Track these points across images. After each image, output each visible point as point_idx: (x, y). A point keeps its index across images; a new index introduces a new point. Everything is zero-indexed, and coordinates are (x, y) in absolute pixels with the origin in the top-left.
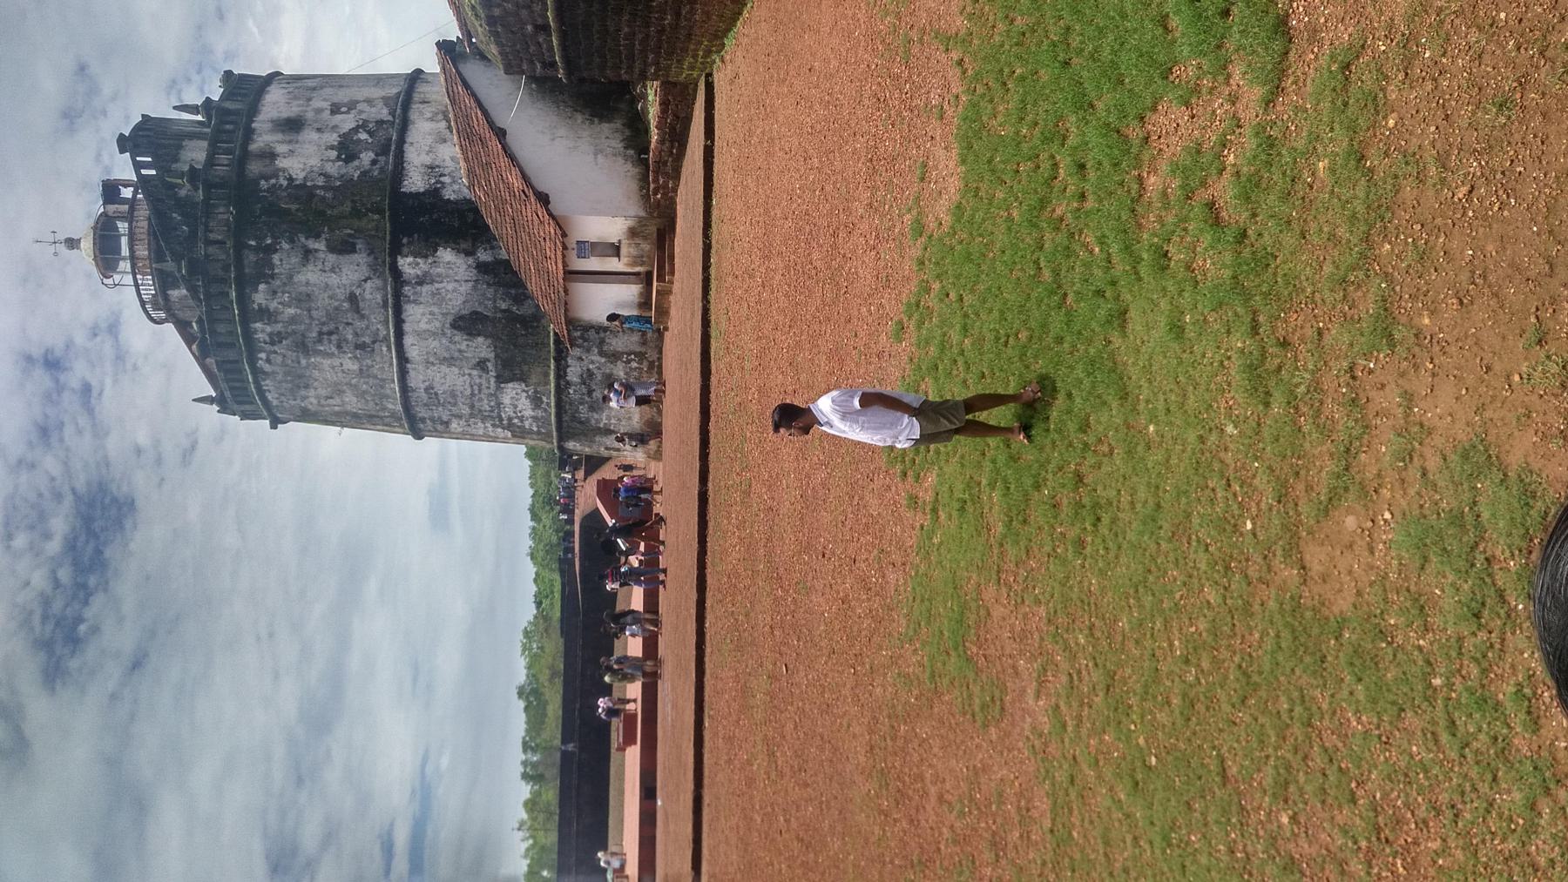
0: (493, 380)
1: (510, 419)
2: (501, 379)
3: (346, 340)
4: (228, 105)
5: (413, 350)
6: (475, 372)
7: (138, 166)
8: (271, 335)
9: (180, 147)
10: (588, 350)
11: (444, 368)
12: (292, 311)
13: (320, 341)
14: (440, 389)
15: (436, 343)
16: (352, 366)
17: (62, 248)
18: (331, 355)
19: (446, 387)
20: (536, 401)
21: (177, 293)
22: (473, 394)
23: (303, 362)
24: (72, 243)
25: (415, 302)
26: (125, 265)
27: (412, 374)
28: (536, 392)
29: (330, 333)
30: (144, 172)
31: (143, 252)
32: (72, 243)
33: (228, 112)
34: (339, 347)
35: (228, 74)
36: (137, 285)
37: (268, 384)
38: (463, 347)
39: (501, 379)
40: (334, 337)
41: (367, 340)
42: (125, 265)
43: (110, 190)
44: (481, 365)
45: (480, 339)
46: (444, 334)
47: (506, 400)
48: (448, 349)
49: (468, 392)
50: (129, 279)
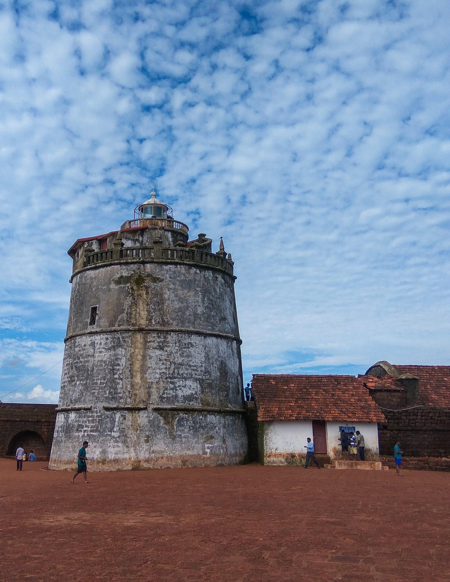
0: (200, 377)
2: (201, 382)
3: (211, 311)
5: (210, 341)
6: (203, 369)
8: (208, 278)
11: (203, 354)
13: (209, 299)
14: (192, 350)
15: (215, 353)
16: (200, 310)
18: (203, 301)
19: (193, 353)
22: (190, 366)
23: (198, 289)
25: (227, 346)
27: (199, 338)
29: (213, 305)
38: (215, 365)
44: (207, 372)
45: (219, 374)
46: (219, 357)
47: (188, 383)
48: (213, 358)
49: (191, 363)
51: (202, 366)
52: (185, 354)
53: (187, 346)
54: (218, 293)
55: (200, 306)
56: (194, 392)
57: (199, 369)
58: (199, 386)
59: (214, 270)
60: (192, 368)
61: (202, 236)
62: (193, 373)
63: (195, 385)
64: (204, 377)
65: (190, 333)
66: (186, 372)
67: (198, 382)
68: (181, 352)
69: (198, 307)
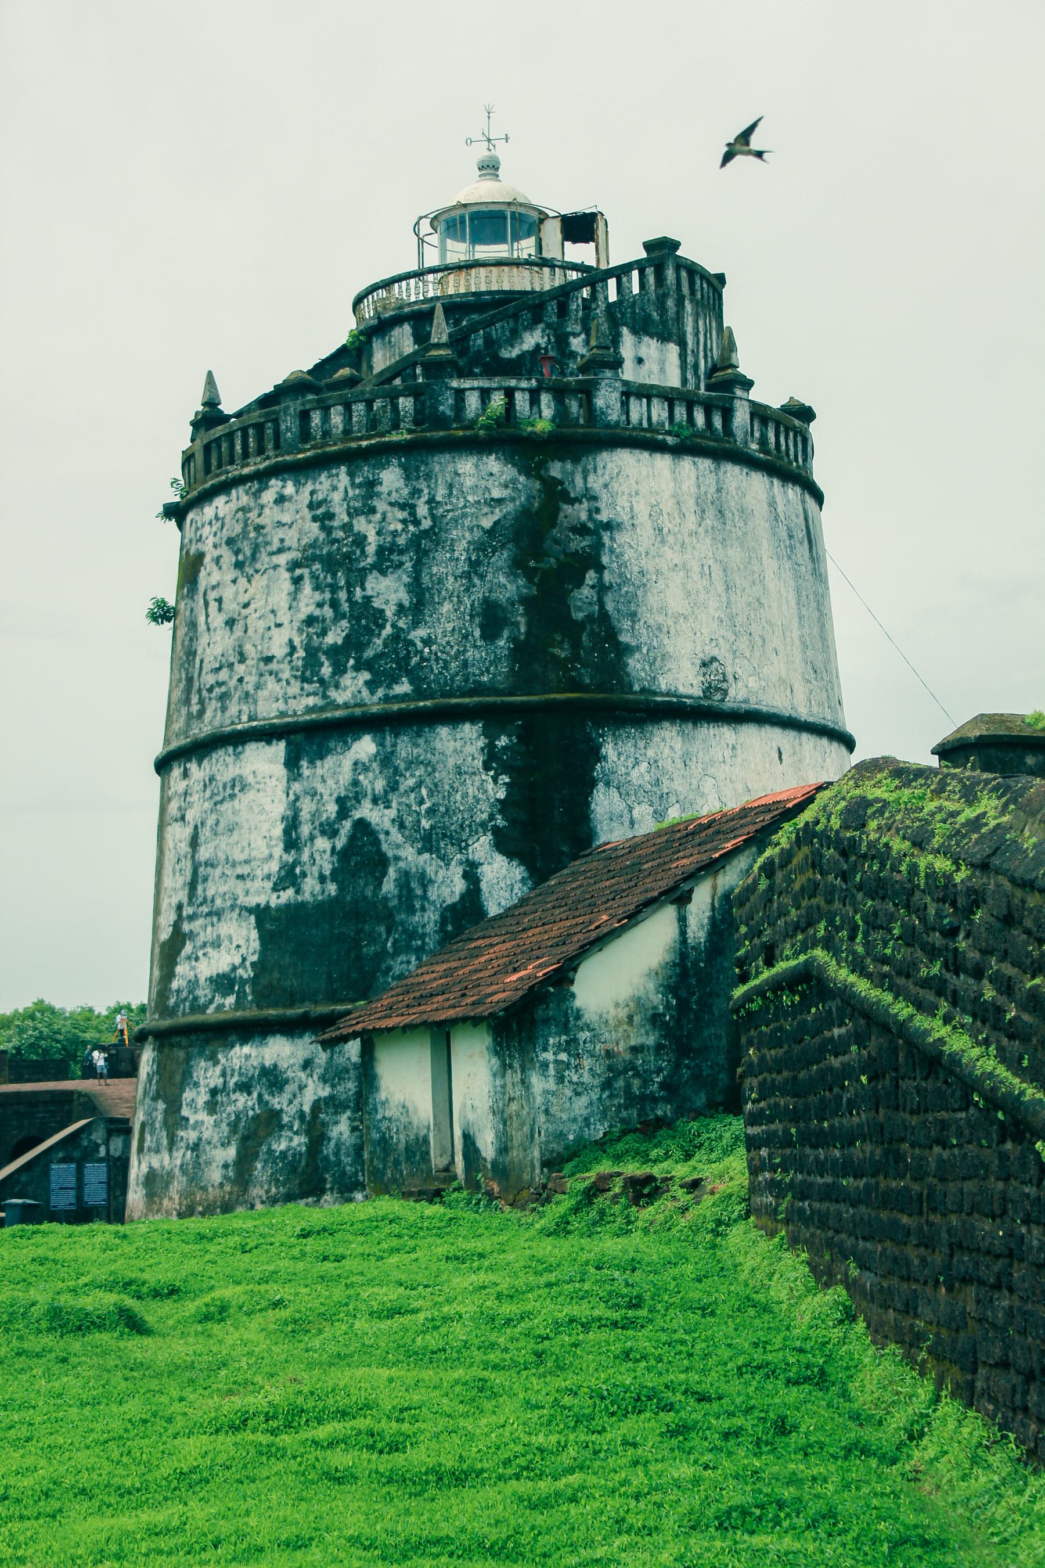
0: (261, 900)
1: (192, 935)
4: (741, 417)
6: (274, 867)
7: (621, 272)
9: (664, 338)
10: (323, 1079)
12: (372, 538)
17: (481, 152)
20: (223, 983)
21: (404, 340)
23: (283, 559)
24: (490, 168)
26: (458, 251)
28: (243, 982)
29: (334, 604)
30: (612, 283)
31: (481, 282)
32: (490, 168)
33: (728, 415)
34: (310, 621)
35: (806, 414)
36: (419, 274)
37: (240, 496)
39: (261, 914)
40: (328, 612)
41: (326, 670)
42: (458, 251)
43: (581, 227)
44: (289, 877)
50: (432, 259)
51: (271, 856)
52: (222, 825)
53: (229, 791)
54: (371, 549)
55: (279, 625)
56: (237, 961)
57: (259, 873)
58: (254, 934)
59: (351, 458)
60: (239, 871)
61: (661, 251)
62: (239, 888)
63: (244, 932)
64: (275, 895)
65: (236, 739)
66: (223, 889)
67: (253, 918)
68: (214, 816)
69: (275, 631)
